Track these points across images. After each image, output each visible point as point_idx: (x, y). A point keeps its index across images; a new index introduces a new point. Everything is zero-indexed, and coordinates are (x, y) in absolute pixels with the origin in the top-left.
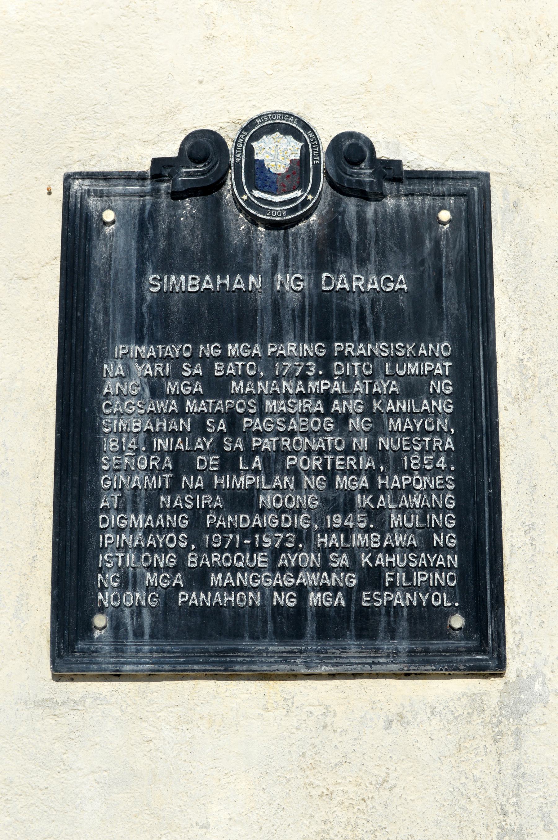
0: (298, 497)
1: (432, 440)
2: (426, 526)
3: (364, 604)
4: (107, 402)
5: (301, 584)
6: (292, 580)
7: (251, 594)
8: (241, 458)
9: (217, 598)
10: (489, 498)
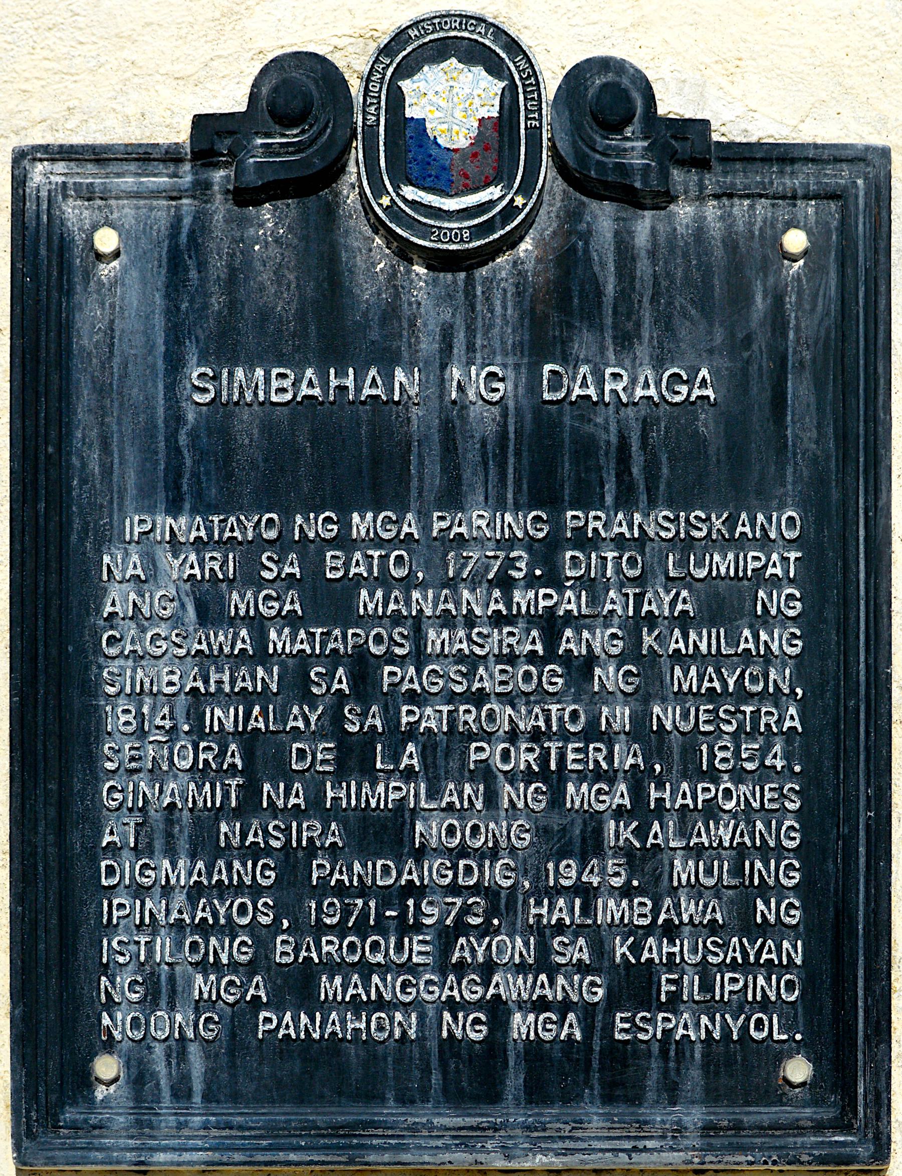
0: (492, 825)
1: (759, 710)
2: (743, 884)
3: (618, 1036)
4: (111, 633)
5: (497, 997)
6: (478, 988)
7: (399, 1017)
8: (379, 747)
9: (333, 1023)
10: (868, 827)
